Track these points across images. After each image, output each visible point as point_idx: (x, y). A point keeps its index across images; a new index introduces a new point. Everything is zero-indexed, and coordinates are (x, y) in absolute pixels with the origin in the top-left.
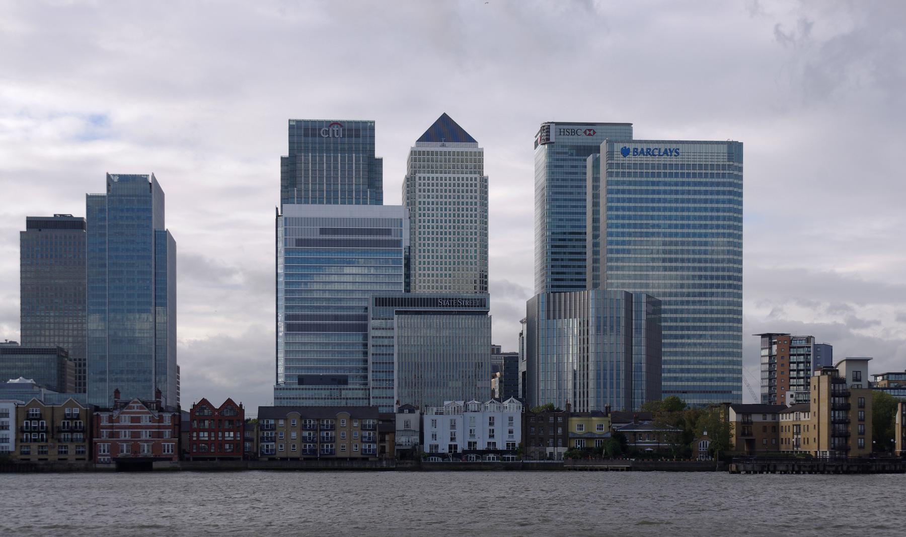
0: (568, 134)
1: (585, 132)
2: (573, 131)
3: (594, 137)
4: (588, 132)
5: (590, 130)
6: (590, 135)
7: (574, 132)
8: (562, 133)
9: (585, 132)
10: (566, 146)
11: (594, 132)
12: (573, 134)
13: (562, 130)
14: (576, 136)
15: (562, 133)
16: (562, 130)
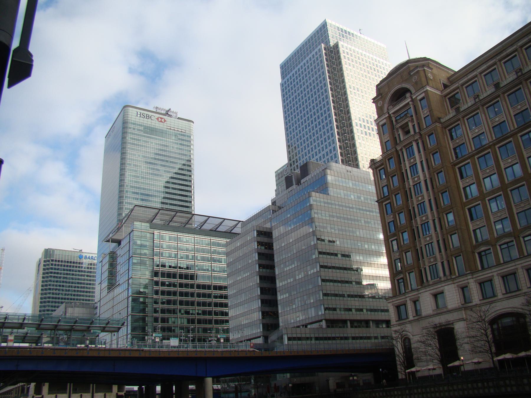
0: (143, 117)
1: (158, 119)
2: (148, 116)
3: (165, 124)
4: (160, 120)
5: (161, 118)
6: (161, 121)
7: (148, 117)
8: (139, 116)
9: (158, 119)
10: (141, 126)
11: (165, 121)
12: (148, 118)
13: (139, 113)
14: (149, 120)
15: (139, 116)
16: (139, 113)
